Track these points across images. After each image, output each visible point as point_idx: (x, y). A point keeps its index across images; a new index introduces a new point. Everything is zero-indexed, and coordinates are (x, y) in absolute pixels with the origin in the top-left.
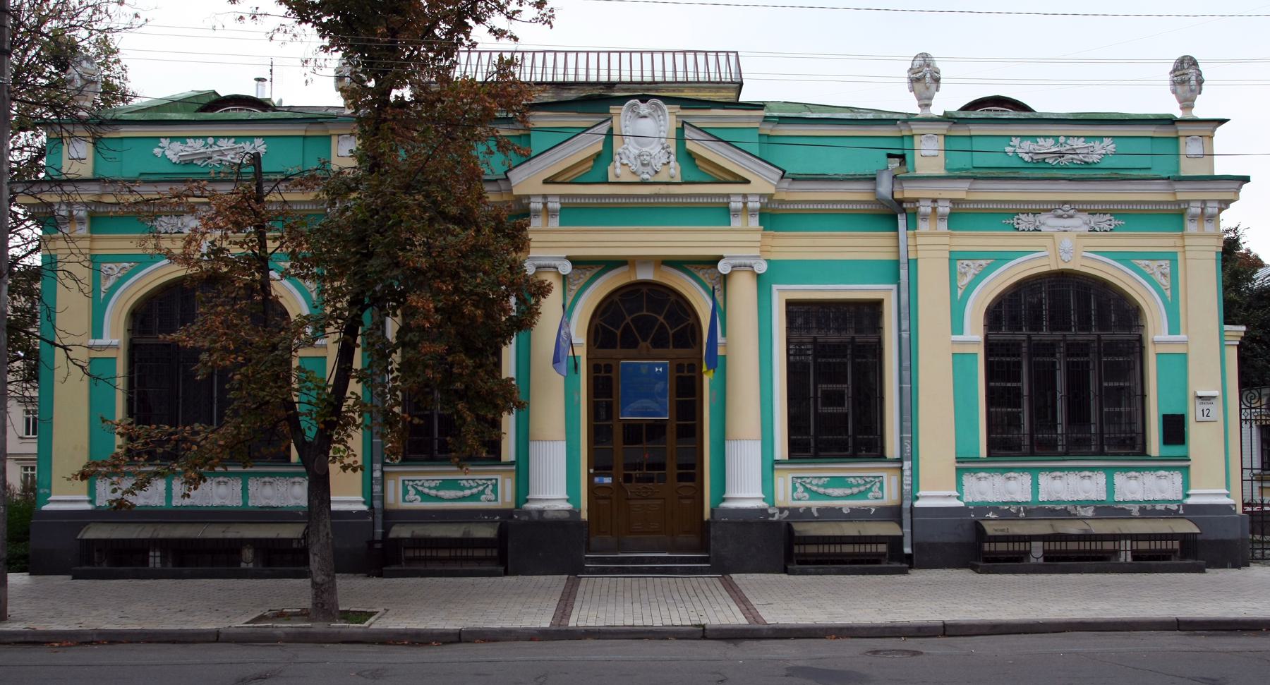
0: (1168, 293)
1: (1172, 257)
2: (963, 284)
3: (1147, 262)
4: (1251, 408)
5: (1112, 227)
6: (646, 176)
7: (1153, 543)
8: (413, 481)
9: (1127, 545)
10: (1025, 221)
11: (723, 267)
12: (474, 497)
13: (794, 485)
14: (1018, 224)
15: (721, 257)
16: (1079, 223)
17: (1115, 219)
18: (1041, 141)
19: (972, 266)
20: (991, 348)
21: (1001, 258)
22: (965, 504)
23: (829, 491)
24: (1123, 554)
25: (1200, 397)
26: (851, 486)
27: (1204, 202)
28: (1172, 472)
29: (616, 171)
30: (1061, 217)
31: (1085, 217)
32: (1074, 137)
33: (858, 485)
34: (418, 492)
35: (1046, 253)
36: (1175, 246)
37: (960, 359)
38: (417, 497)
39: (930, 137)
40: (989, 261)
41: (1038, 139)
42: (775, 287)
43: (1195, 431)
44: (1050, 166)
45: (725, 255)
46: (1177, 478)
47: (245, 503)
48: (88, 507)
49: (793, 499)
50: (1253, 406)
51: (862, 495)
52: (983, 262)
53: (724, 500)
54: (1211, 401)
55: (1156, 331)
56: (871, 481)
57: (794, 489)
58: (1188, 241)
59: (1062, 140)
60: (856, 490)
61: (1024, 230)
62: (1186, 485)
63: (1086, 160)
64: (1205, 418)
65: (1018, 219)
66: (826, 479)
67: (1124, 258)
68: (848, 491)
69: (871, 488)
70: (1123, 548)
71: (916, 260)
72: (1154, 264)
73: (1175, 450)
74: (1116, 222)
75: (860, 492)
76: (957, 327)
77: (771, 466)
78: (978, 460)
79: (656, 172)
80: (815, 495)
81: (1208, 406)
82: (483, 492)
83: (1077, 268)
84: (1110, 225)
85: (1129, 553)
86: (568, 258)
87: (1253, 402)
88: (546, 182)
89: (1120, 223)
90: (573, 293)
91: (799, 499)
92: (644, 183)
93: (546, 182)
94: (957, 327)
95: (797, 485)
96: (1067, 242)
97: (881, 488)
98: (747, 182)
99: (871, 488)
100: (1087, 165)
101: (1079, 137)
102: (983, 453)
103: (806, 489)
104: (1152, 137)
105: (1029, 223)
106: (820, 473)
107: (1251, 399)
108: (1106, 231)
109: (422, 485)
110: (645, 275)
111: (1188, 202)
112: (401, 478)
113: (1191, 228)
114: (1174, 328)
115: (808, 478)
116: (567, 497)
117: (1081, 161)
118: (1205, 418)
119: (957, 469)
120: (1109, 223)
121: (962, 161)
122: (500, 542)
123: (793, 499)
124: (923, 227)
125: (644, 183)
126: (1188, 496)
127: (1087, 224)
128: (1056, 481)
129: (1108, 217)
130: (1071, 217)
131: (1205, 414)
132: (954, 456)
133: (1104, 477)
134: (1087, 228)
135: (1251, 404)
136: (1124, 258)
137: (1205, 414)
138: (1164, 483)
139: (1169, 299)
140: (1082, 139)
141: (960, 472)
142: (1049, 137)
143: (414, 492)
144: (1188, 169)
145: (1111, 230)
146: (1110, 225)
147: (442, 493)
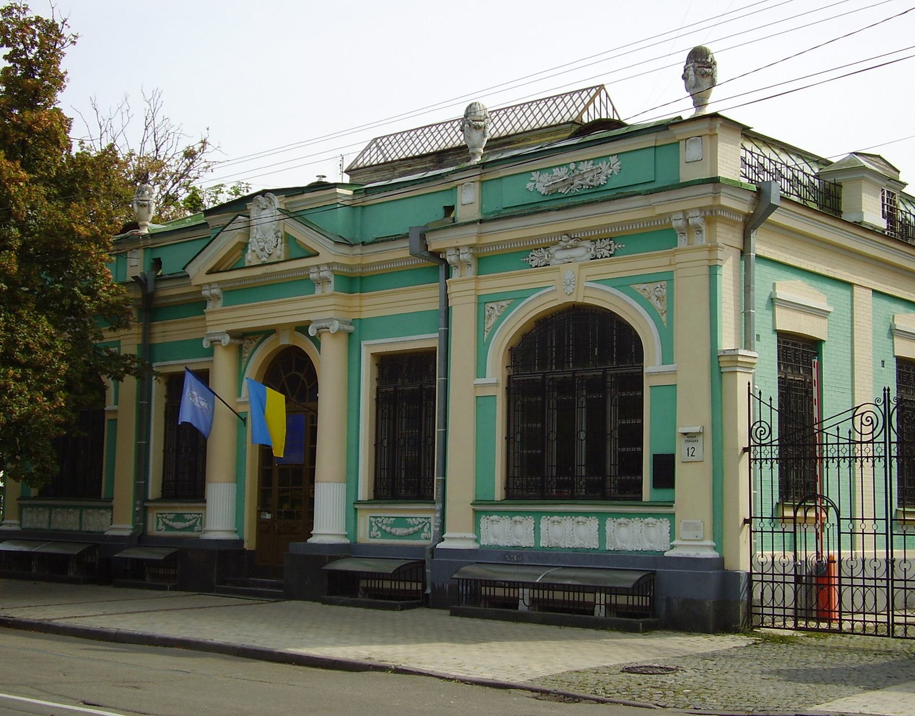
0: (664, 318)
1: (669, 278)
2: (488, 326)
3: (644, 286)
4: (761, 445)
5: (611, 252)
6: (264, 259)
7: (630, 598)
8: (161, 514)
9: (601, 598)
10: (537, 258)
11: (312, 331)
12: (191, 528)
13: (371, 523)
14: (532, 260)
15: (310, 322)
16: (582, 253)
17: (615, 244)
18: (556, 171)
19: (496, 308)
20: (514, 389)
21: (518, 297)
22: (481, 547)
23: (393, 531)
24: (597, 607)
25: (685, 434)
26: (408, 526)
27: (684, 212)
28: (661, 519)
29: (250, 258)
30: (565, 249)
31: (587, 244)
32: (583, 161)
33: (414, 525)
34: (164, 523)
35: (554, 288)
36: (670, 265)
37: (482, 402)
38: (164, 527)
39: (467, 185)
40: (509, 302)
41: (554, 170)
42: (363, 343)
43: (681, 472)
44: (563, 196)
45: (311, 320)
46: (665, 524)
47: (81, 528)
48: (471, 545)
49: (370, 537)
50: (763, 442)
51: (416, 534)
52: (504, 303)
53: (311, 536)
54: (696, 439)
55: (652, 363)
56: (424, 522)
57: (371, 527)
58: (679, 258)
59: (572, 166)
60: (411, 530)
61: (536, 267)
62: (672, 534)
63: (592, 184)
64: (691, 458)
65: (532, 256)
66: (392, 519)
67: (622, 284)
68: (405, 531)
69: (423, 528)
70: (598, 602)
71: (451, 307)
72: (650, 287)
73: (663, 494)
74: (616, 246)
75: (415, 532)
76: (480, 371)
77: (354, 506)
78: (493, 503)
79: (270, 255)
80: (386, 534)
81: (690, 445)
82: (195, 524)
83: (580, 300)
84: (610, 250)
85: (603, 607)
86: (229, 332)
87: (763, 437)
88: (210, 272)
89: (620, 246)
90: (245, 360)
91: (374, 537)
92: (264, 264)
93: (210, 272)
94: (480, 371)
95: (373, 524)
96: (569, 272)
97: (429, 529)
98: (318, 254)
99: (423, 528)
100: (597, 189)
101: (588, 160)
102: (499, 494)
103: (380, 529)
104: (655, 147)
105: (541, 258)
106: (391, 512)
107: (761, 434)
108: (606, 257)
109: (165, 518)
110: (285, 340)
111: (670, 214)
112: (156, 511)
113: (682, 242)
114: (668, 357)
115: (381, 517)
116: (236, 529)
117: (589, 186)
118: (691, 458)
119: (475, 511)
120: (608, 248)
121: (493, 206)
122: (170, 561)
123: (370, 537)
124: (455, 275)
125: (264, 264)
126: (672, 547)
127: (587, 252)
128: (622, 528)
129: (607, 242)
130: (573, 247)
131: (690, 455)
132: (471, 498)
133: (598, 523)
134: (589, 256)
135: (760, 439)
136: (622, 284)
137: (690, 455)
138: (582, 530)
139: (665, 324)
140: (591, 162)
141: (477, 514)
142: (562, 165)
143: (376, 528)
144: (687, 174)
145: (611, 255)
146: (610, 250)
147: (175, 524)
